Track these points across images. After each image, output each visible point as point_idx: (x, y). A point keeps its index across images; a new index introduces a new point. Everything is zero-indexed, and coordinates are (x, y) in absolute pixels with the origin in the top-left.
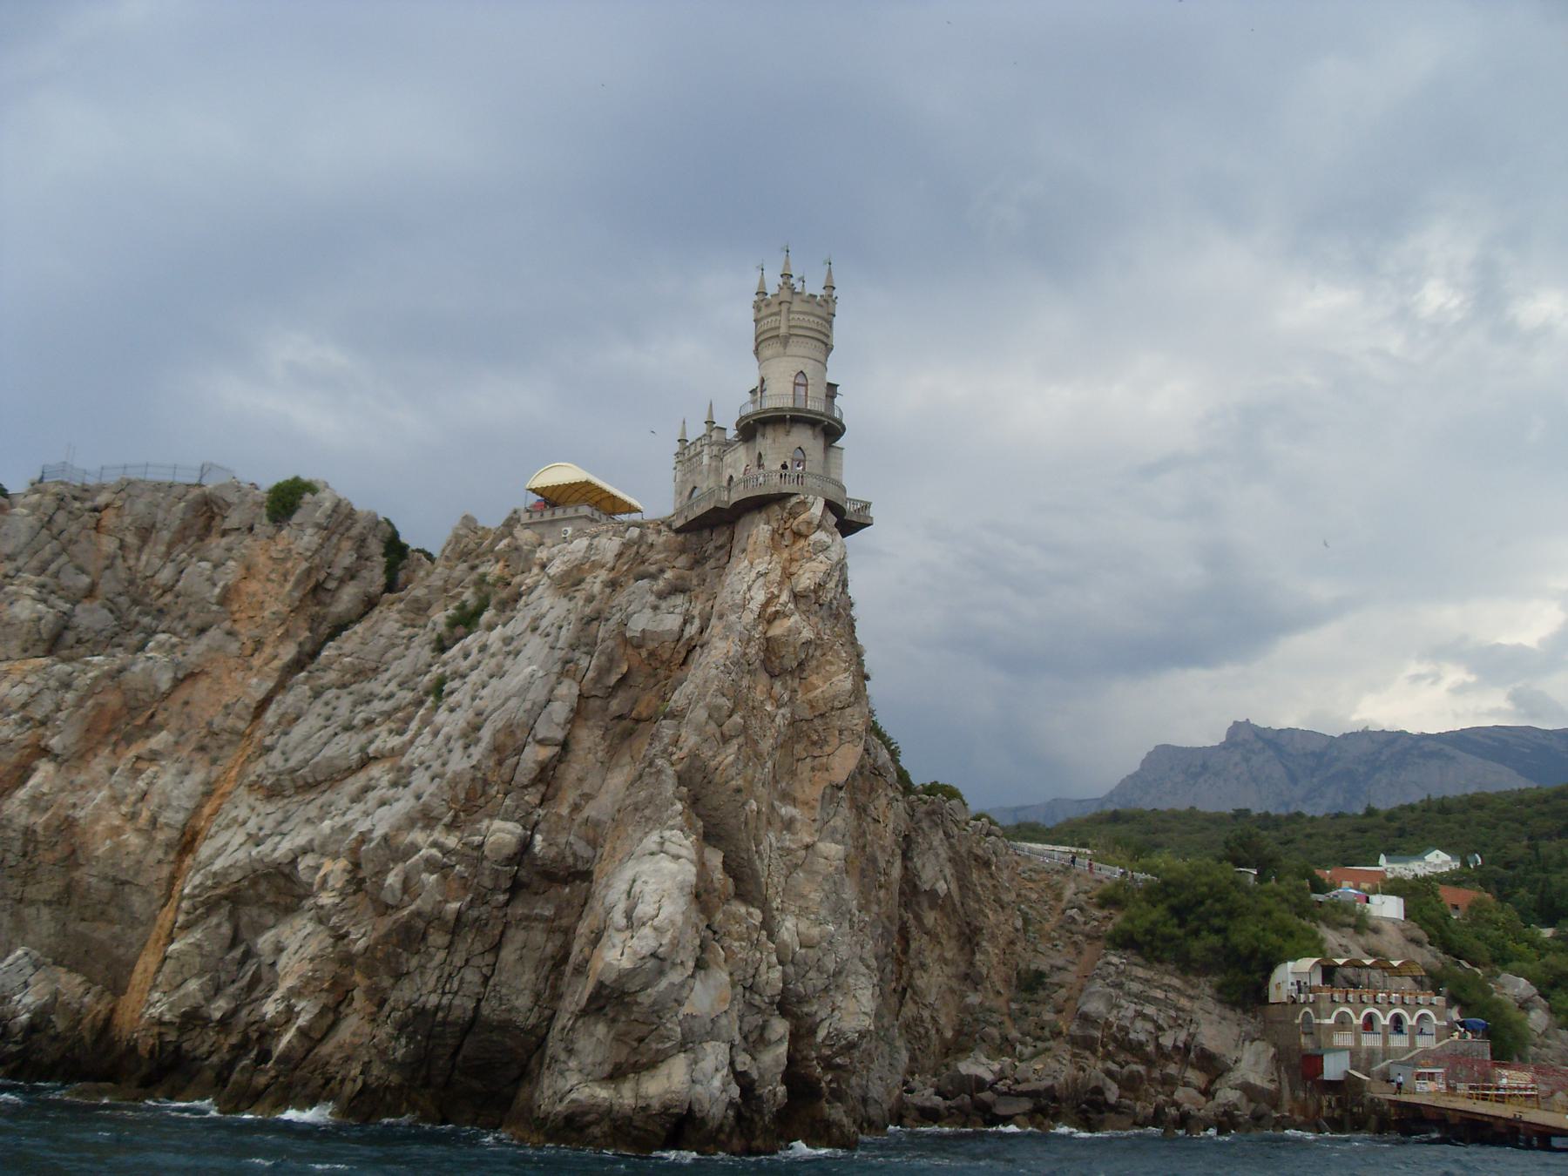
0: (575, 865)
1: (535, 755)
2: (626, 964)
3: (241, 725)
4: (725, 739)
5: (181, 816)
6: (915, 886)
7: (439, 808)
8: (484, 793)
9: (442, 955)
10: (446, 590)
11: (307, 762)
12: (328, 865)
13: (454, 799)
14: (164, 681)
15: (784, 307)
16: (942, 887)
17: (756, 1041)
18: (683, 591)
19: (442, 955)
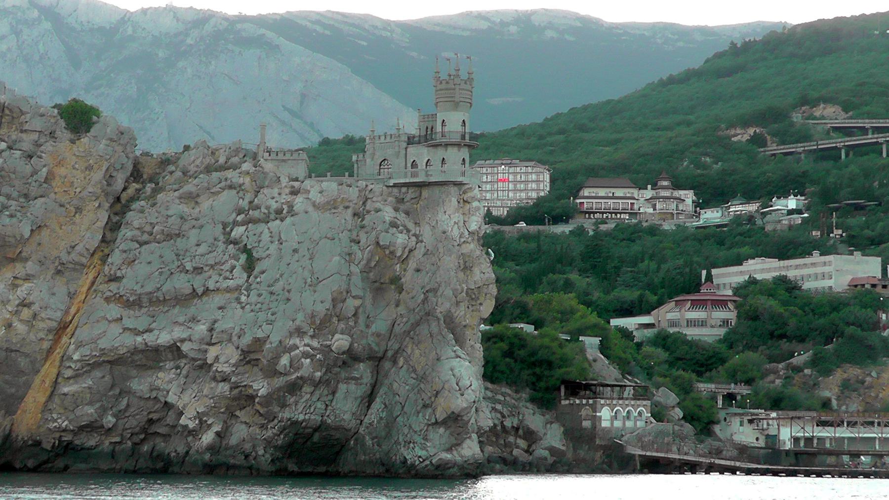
2: (465, 405)
3: (84, 260)
5: (59, 314)
7: (306, 328)
8: (330, 321)
11: (158, 289)
13: (313, 323)
14: (27, 234)
15: (457, 87)
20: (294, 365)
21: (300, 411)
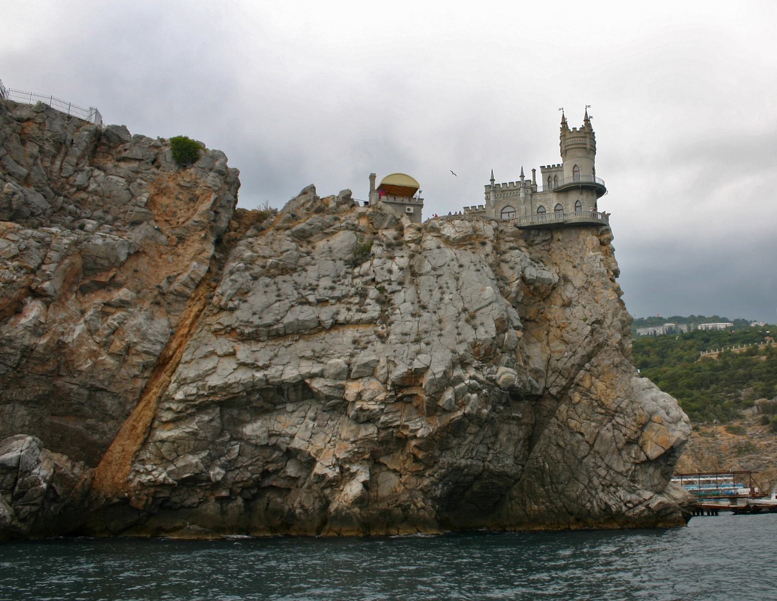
0: (531, 392)
3: (188, 291)
5: (158, 347)
10: (322, 229)
11: (278, 321)
13: (478, 353)
19: (471, 438)
20: (459, 401)
21: (462, 454)
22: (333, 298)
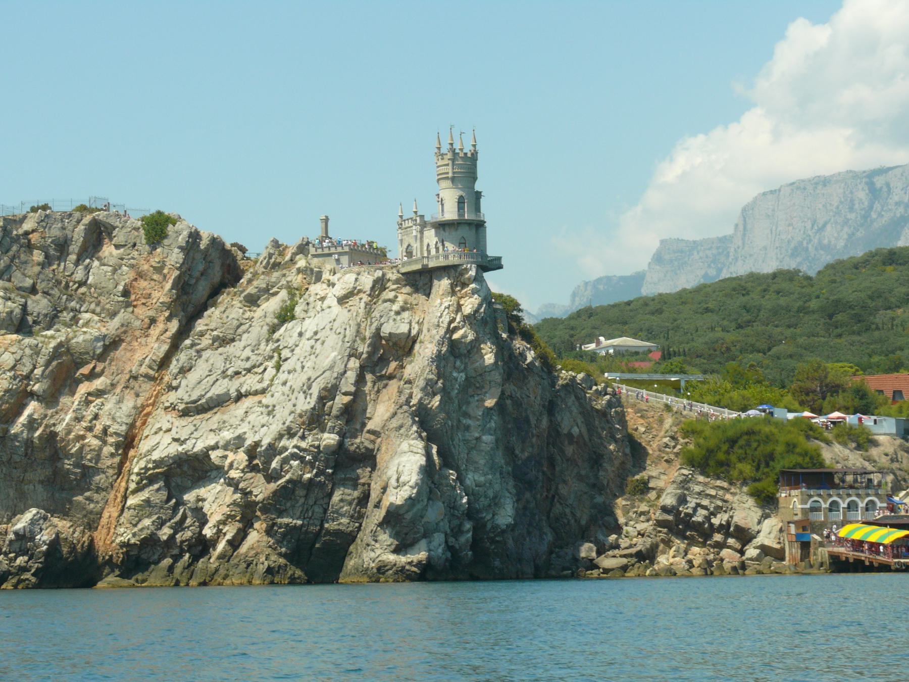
1: (341, 400)
4: (434, 394)
5: (124, 428)
6: (558, 432)
9: (302, 500)
10: (269, 290)
12: (231, 456)
16: (575, 431)
17: (457, 532)
18: (408, 309)
19: (302, 500)
22: (245, 369)
